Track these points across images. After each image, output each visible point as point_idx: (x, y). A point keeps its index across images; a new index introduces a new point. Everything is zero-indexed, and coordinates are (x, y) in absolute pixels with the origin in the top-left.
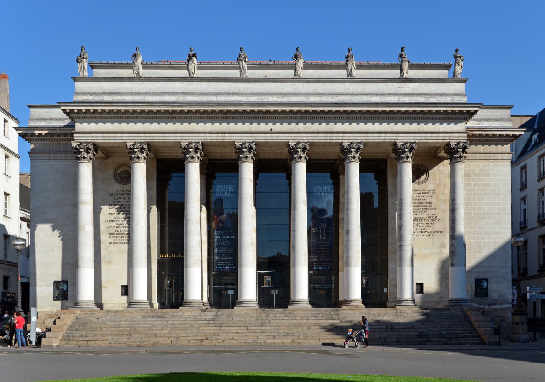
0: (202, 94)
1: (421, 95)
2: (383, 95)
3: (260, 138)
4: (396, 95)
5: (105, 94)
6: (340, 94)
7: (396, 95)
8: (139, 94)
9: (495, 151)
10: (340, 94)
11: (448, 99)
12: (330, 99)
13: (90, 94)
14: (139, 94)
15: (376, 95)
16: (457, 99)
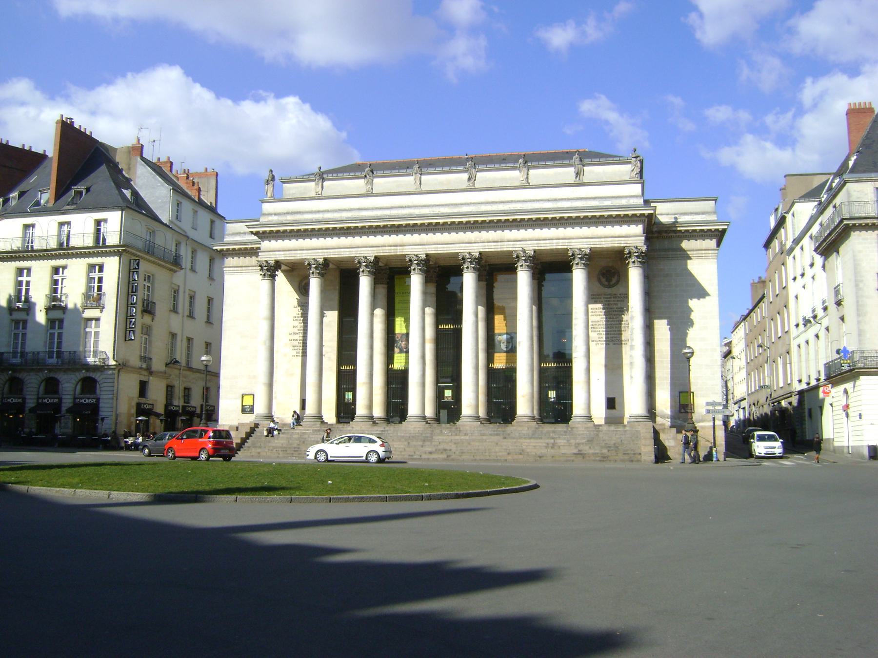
0: (377, 209)
1: (595, 198)
2: (555, 200)
3: (432, 250)
4: (568, 199)
5: (288, 213)
6: (512, 202)
7: (568, 199)
8: (319, 212)
9: (698, 247)
10: (512, 202)
11: (624, 202)
12: (501, 207)
13: (275, 214)
14: (319, 212)
15: (549, 200)
16: (633, 201)
